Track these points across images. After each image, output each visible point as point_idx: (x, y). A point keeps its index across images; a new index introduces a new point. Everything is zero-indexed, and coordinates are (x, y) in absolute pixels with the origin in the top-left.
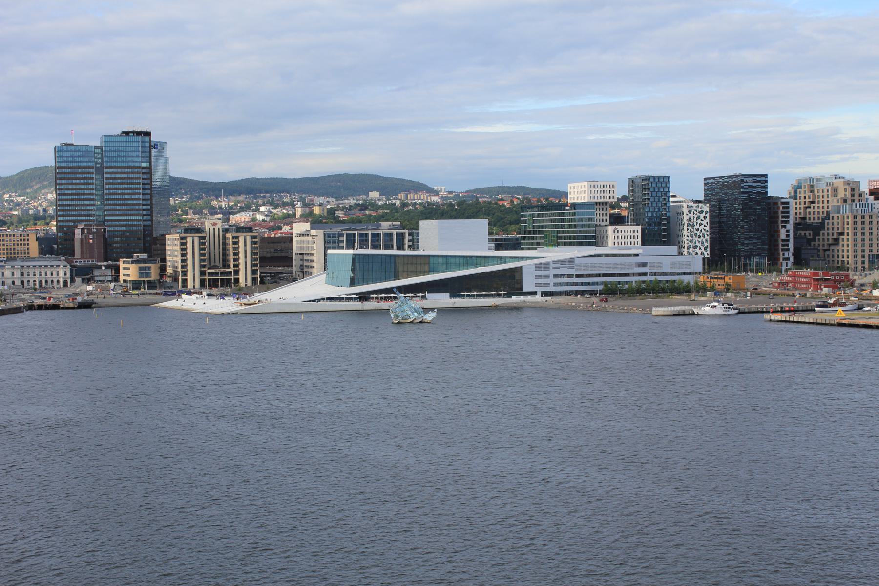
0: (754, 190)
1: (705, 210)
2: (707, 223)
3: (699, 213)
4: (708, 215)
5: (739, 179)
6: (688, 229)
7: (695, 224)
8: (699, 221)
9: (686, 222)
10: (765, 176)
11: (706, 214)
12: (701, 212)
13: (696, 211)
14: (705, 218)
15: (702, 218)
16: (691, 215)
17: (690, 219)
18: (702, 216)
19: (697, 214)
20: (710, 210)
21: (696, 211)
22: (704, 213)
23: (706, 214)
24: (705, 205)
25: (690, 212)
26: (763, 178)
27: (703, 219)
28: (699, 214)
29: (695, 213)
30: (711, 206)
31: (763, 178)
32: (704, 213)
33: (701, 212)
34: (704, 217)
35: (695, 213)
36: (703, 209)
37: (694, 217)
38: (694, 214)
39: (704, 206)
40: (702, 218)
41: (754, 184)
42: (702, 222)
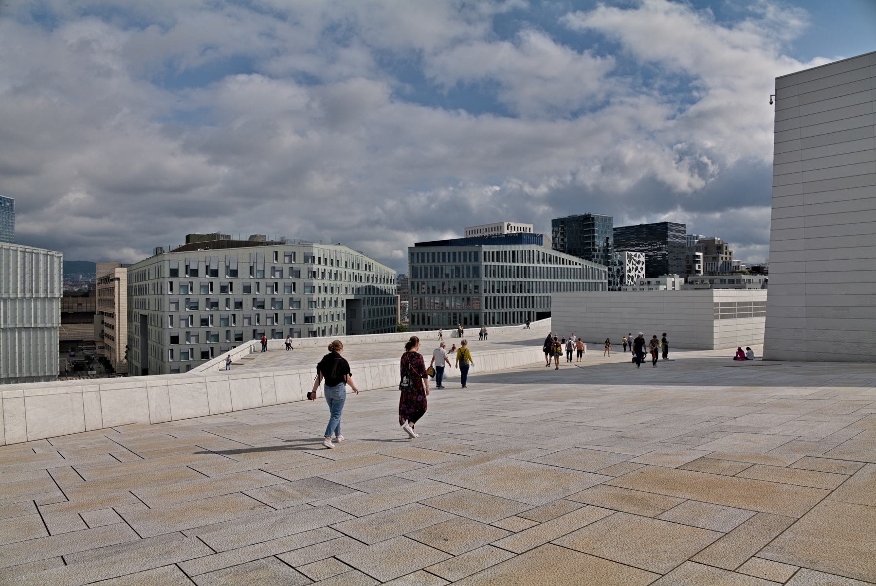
0: (677, 240)
1: (641, 261)
2: (643, 275)
3: (637, 263)
4: (644, 266)
5: (663, 228)
6: (628, 282)
7: (634, 277)
8: (637, 273)
9: (627, 274)
10: (683, 226)
11: (642, 265)
12: (638, 262)
13: (635, 260)
14: (642, 269)
15: (639, 269)
16: (631, 265)
17: (630, 271)
18: (640, 266)
19: (635, 265)
20: (645, 261)
21: (635, 260)
22: (641, 263)
23: (642, 265)
24: (642, 254)
25: (630, 261)
26: (683, 228)
27: (640, 271)
28: (637, 265)
29: (634, 263)
30: (646, 256)
31: (683, 228)
32: (641, 263)
33: (638, 262)
34: (641, 268)
35: (634, 263)
36: (640, 259)
37: (633, 268)
38: (633, 264)
39: (641, 255)
40: (639, 269)
41: (677, 234)
42: (639, 274)
